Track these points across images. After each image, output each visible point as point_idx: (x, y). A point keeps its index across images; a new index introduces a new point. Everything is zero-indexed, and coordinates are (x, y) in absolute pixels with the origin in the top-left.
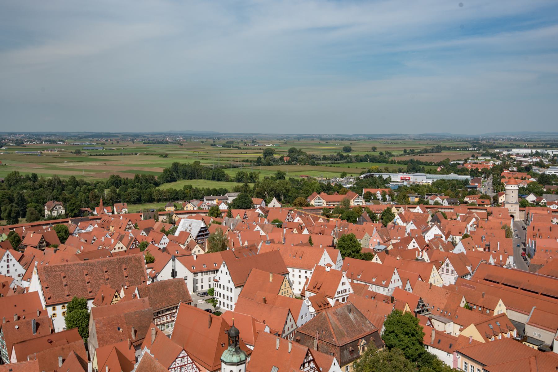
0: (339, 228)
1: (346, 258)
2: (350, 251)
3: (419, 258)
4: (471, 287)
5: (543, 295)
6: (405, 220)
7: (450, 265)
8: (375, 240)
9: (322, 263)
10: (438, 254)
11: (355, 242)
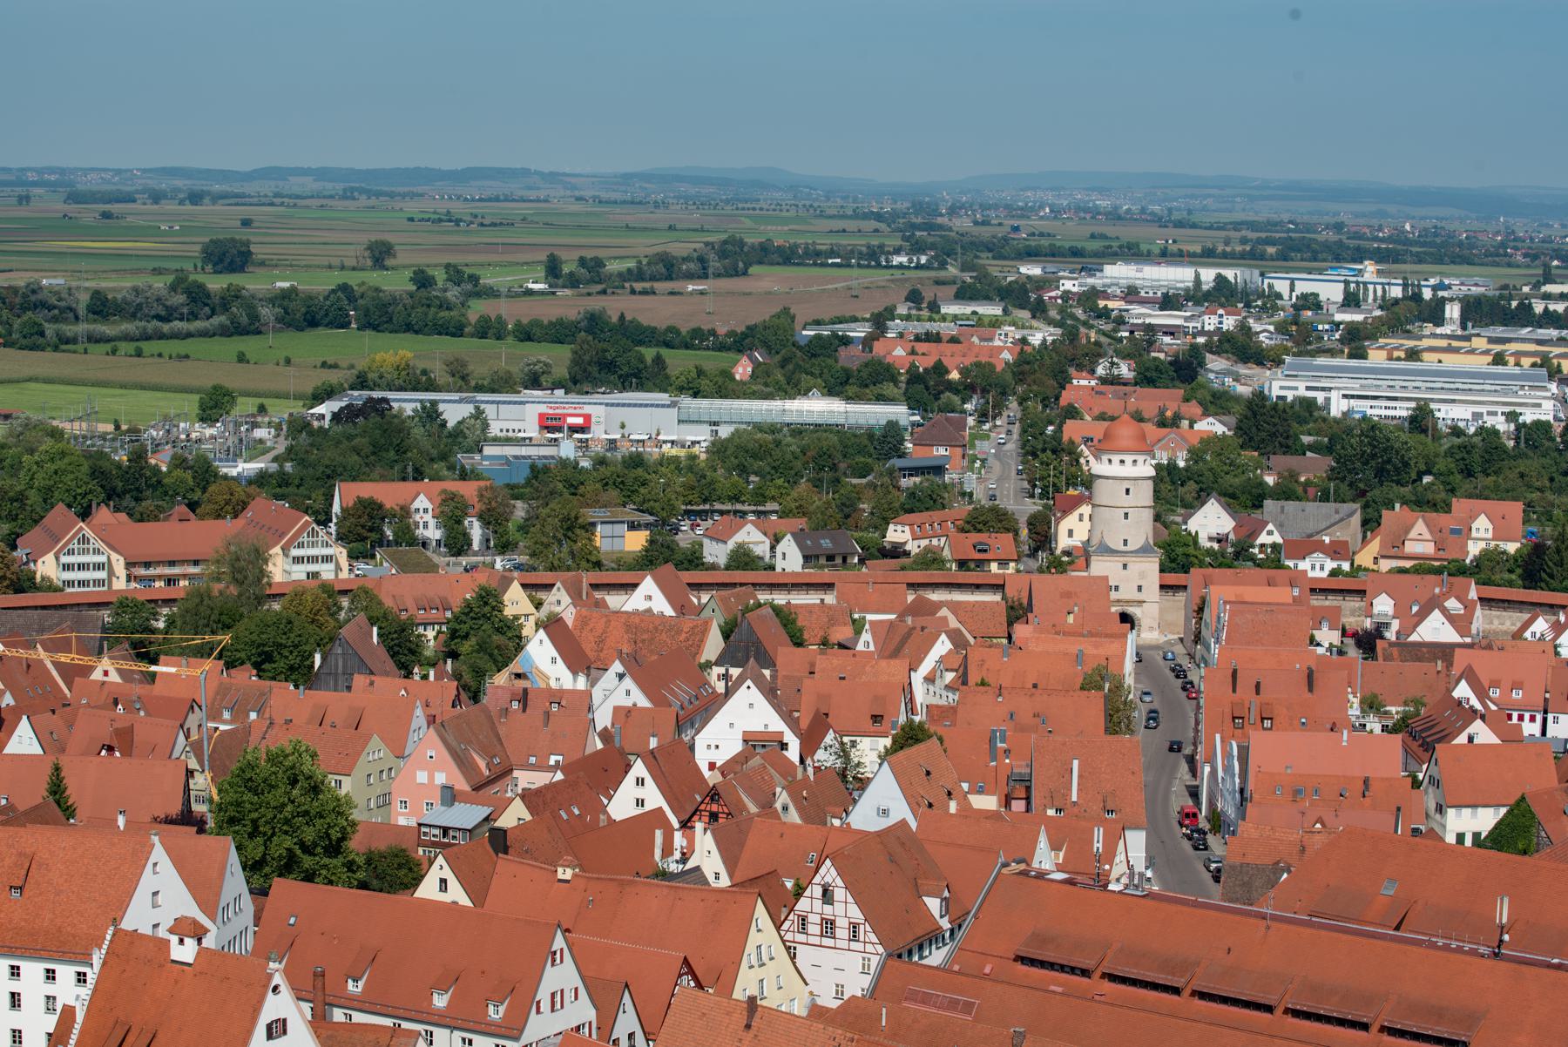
0: (215, 716)
1: (280, 886)
2: (289, 842)
3: (674, 867)
4: (953, 1005)
5: (1297, 1013)
6: (578, 658)
7: (840, 893)
8: (422, 777)
9: (138, 917)
10: (774, 833)
11: (315, 789)
